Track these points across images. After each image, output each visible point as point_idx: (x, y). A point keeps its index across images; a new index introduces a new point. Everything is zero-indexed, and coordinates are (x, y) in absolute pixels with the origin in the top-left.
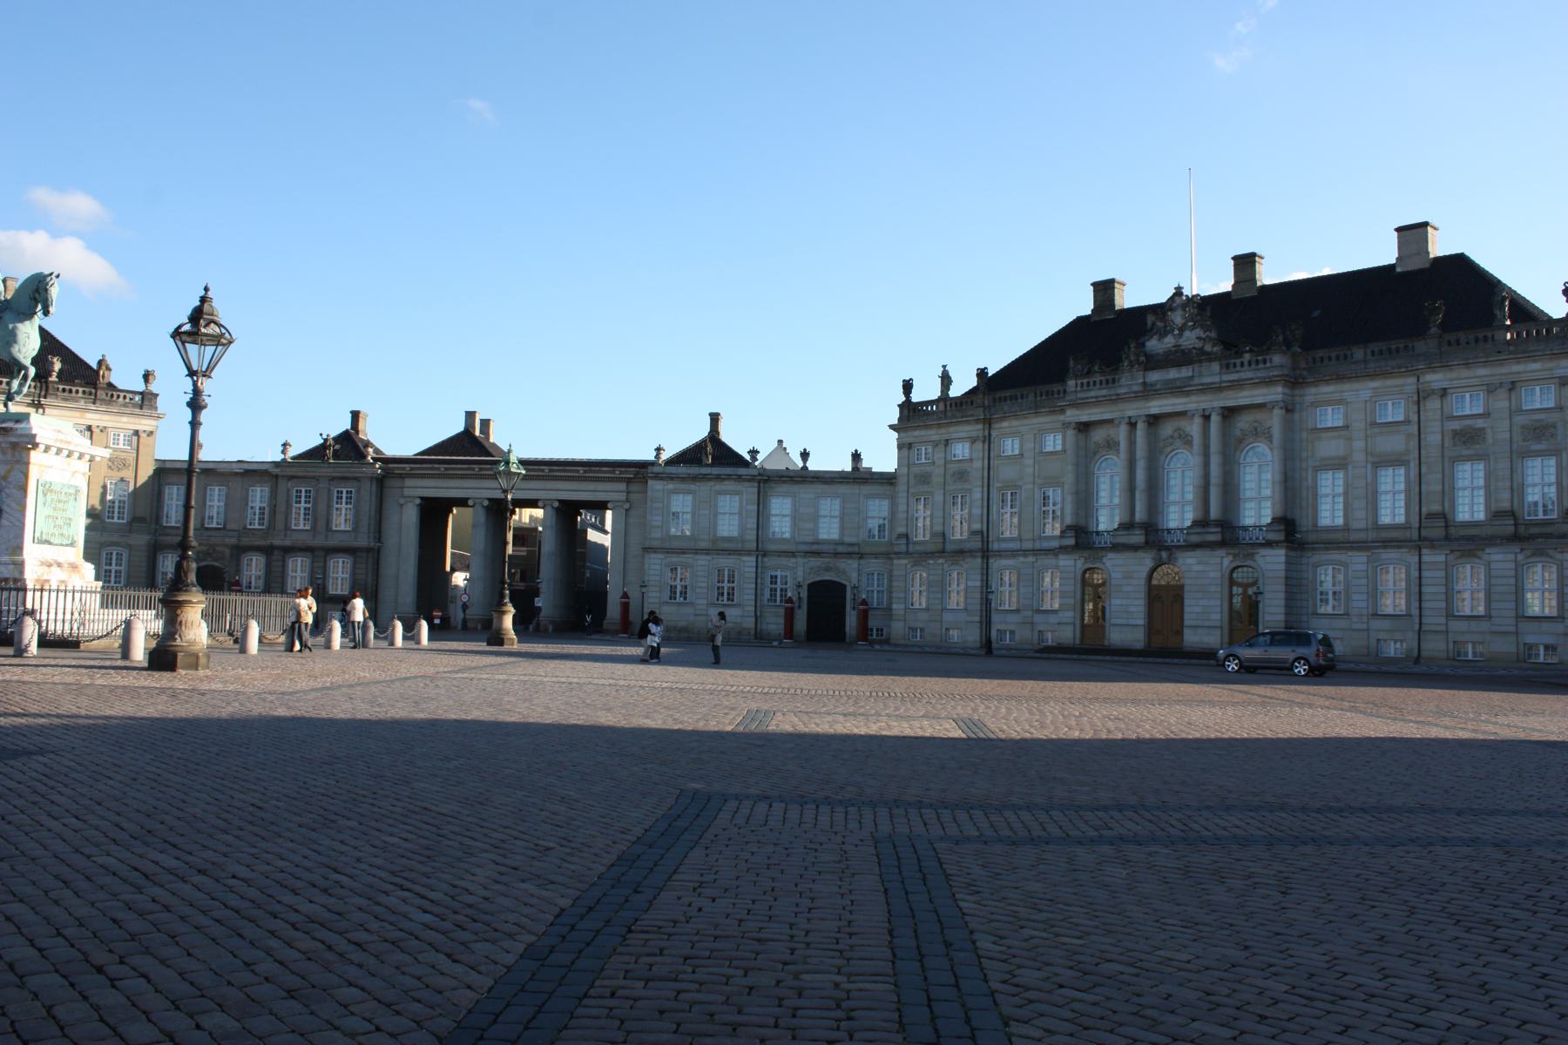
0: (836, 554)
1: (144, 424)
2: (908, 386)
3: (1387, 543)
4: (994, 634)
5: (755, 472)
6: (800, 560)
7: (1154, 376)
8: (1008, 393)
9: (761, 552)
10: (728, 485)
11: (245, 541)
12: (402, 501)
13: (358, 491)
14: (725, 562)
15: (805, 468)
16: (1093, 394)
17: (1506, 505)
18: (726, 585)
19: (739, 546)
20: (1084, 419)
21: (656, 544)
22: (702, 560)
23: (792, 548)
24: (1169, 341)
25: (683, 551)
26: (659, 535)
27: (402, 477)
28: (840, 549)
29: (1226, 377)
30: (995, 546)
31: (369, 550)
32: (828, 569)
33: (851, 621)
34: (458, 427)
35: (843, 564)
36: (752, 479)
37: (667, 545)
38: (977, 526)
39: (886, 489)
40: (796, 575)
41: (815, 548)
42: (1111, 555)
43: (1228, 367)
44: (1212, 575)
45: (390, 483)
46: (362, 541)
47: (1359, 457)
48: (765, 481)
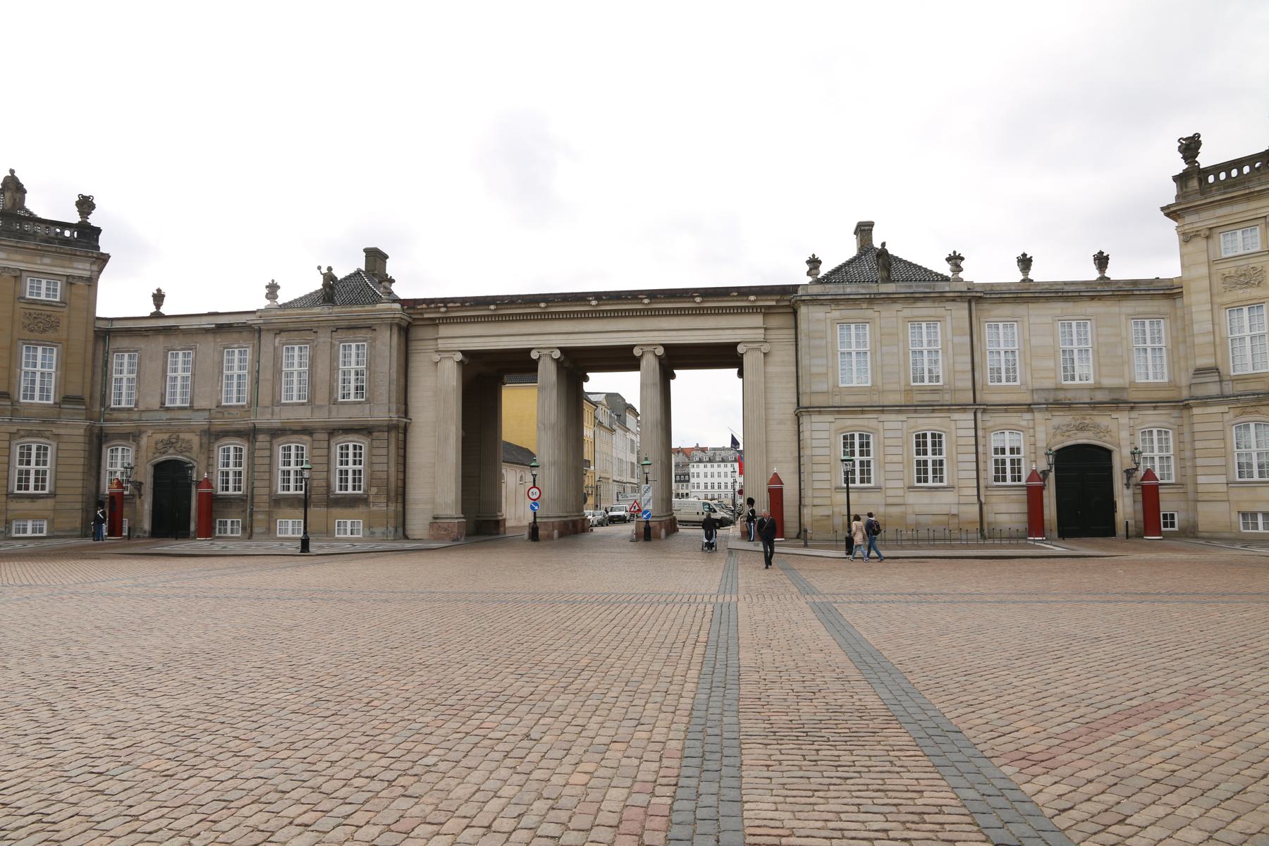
0: (1094, 405)
1: (81, 268)
2: (1190, 147)
6: (1038, 415)
9: (977, 407)
11: (219, 424)
12: (436, 357)
13: (371, 346)
14: (928, 424)
18: (930, 457)
22: (893, 422)
23: (1027, 399)
25: (862, 409)
26: (824, 387)
27: (434, 323)
28: (1100, 396)
31: (391, 428)
32: (1082, 428)
33: (1126, 505)
35: (1104, 420)
37: (837, 401)
39: (1162, 306)
41: (1061, 396)
48: (979, 299)
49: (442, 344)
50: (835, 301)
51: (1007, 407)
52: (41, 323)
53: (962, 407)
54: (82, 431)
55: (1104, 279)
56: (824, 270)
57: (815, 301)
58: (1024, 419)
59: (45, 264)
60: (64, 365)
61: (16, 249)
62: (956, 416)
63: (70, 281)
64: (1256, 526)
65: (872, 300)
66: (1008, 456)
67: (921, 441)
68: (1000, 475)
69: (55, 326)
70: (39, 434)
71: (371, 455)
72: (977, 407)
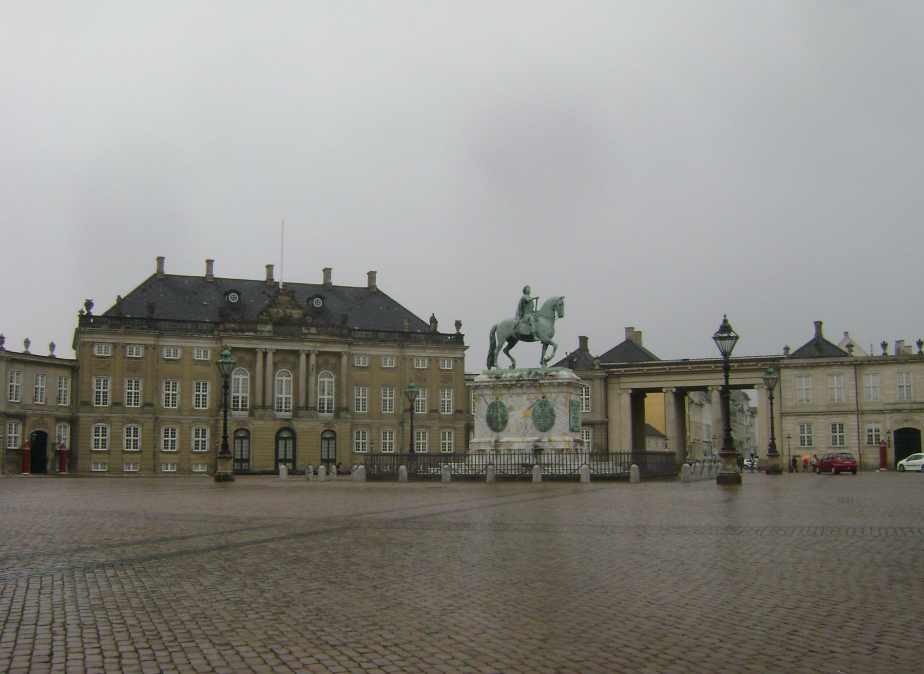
0: (912, 411)
1: (458, 354)
5: (852, 359)
6: (888, 416)
10: (835, 370)
12: (620, 392)
15: (885, 354)
18: (838, 434)
19: (845, 409)
21: (789, 410)
22: (821, 419)
25: (806, 414)
26: (791, 404)
28: (915, 406)
32: (906, 421)
34: (622, 339)
36: (851, 364)
40: (887, 426)
41: (897, 407)
45: (611, 380)
46: (598, 417)
49: (622, 386)
50: (796, 367)
51: (873, 412)
52: (447, 379)
53: (852, 412)
54: (463, 426)
56: (791, 352)
57: (787, 367)
58: (880, 417)
59: (449, 354)
60: (455, 397)
61: (437, 349)
62: (850, 416)
63: (455, 359)
65: (812, 366)
66: (874, 433)
67: (834, 425)
68: (870, 442)
69: (450, 380)
70: (448, 427)
71: (594, 434)
72: (859, 412)
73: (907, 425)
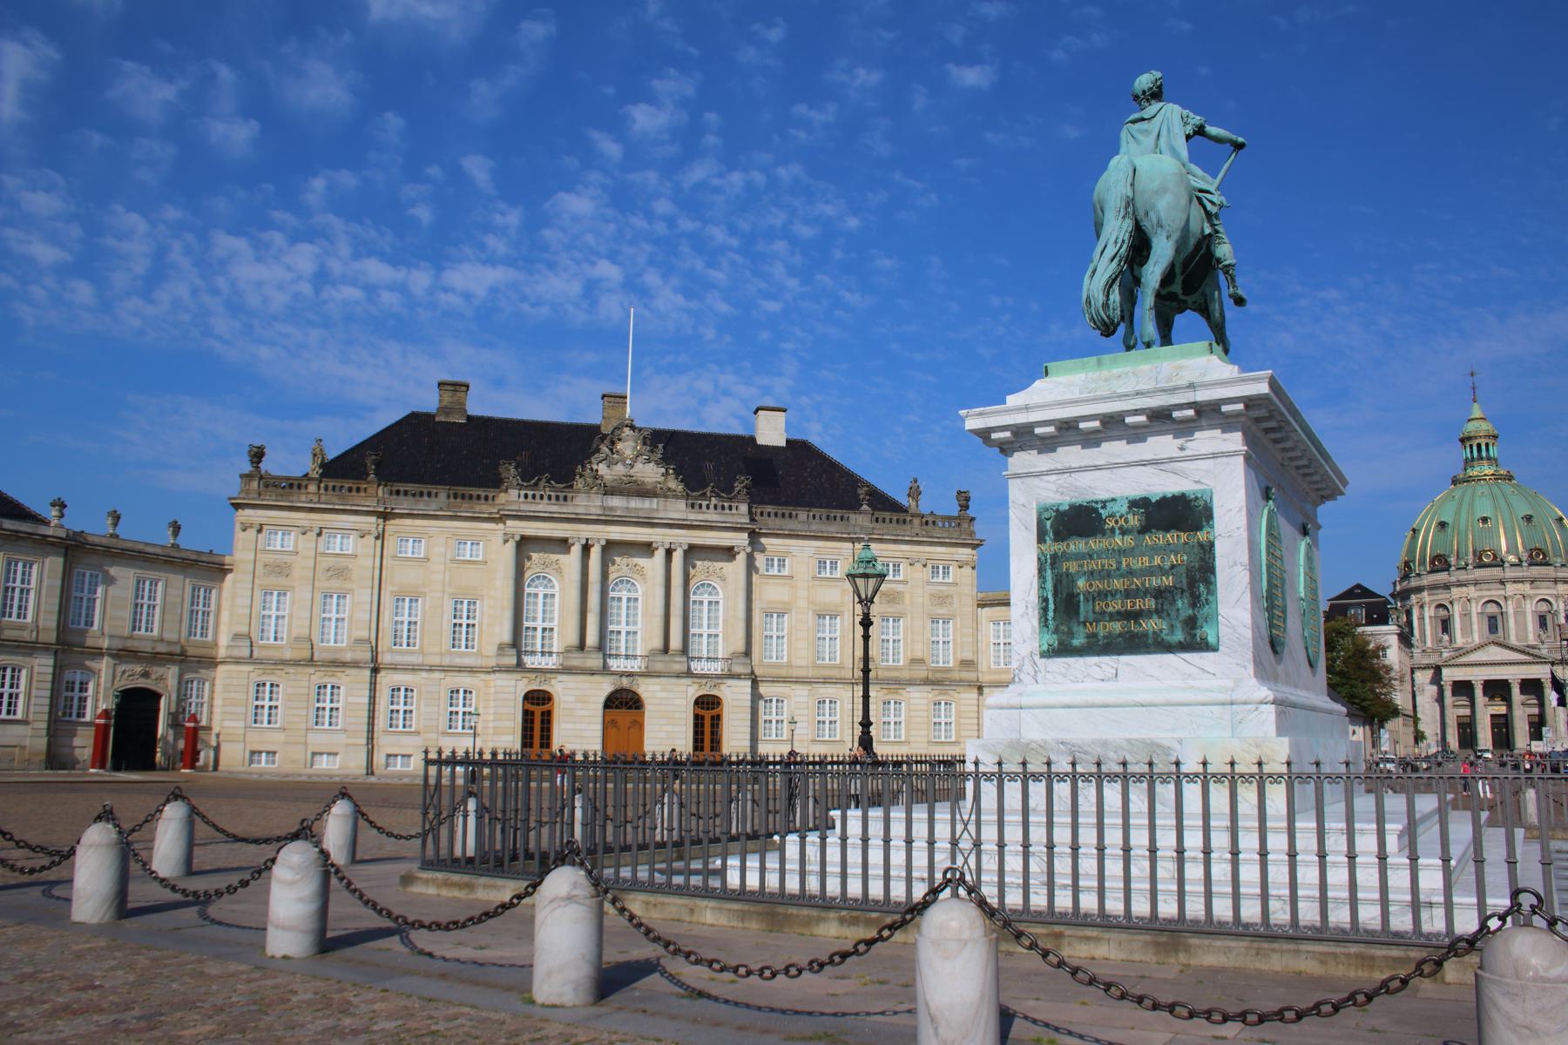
3: (826, 681)
4: (380, 759)
7: (616, 502)
8: (410, 487)
16: (540, 507)
17: (918, 655)
20: (529, 532)
24: (620, 469)
28: (162, 648)
29: (694, 516)
30: (385, 658)
38: (364, 634)
42: (561, 677)
43: (693, 506)
44: (678, 702)
47: (802, 603)
55: (175, 546)
64: (259, 762)
73: (142, 683)
